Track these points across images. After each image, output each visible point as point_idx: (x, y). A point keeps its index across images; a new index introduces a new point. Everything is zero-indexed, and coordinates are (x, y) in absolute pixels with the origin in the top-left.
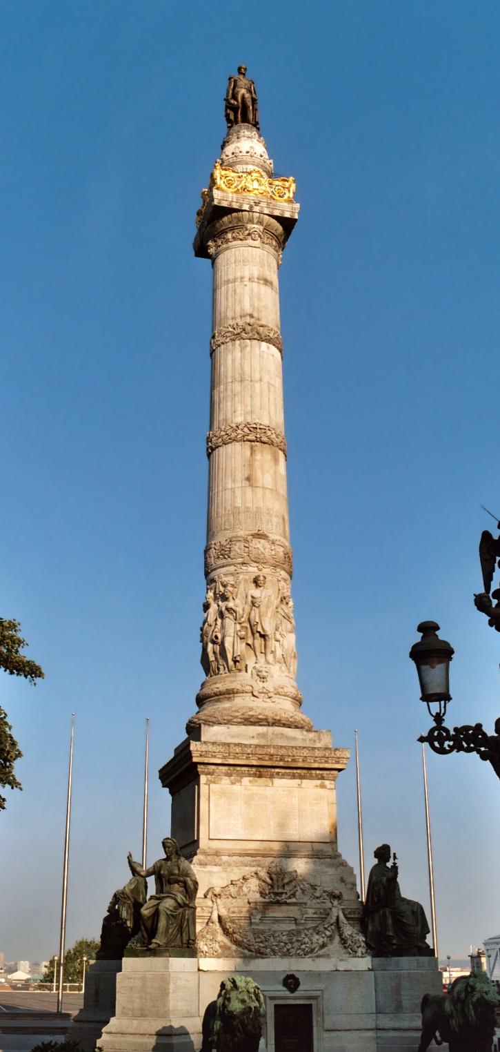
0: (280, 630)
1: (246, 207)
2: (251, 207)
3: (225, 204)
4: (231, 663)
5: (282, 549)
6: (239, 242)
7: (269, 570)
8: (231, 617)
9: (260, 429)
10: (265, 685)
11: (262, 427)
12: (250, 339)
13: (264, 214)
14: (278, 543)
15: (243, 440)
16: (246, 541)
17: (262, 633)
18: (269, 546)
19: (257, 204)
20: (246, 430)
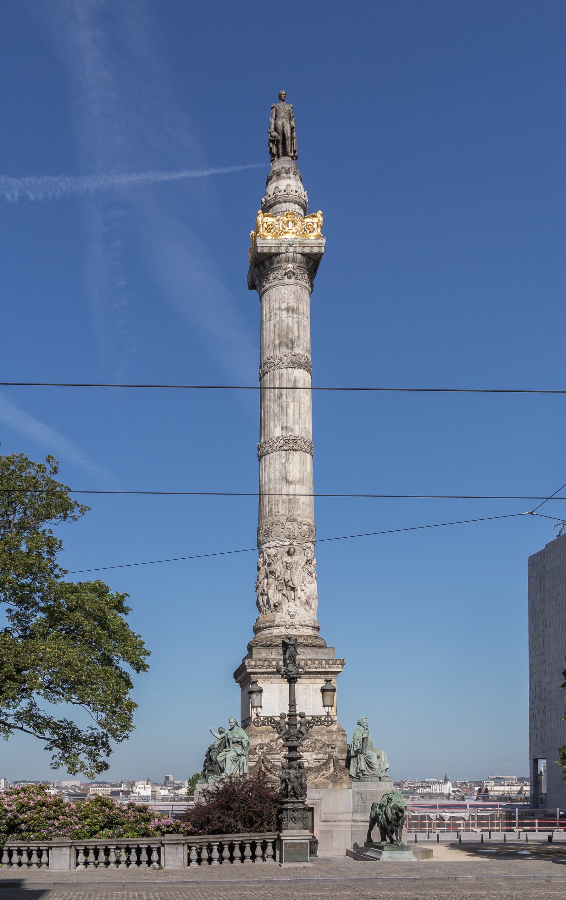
0: (305, 582)
4: (272, 607)
5: (307, 527)
6: (277, 282)
8: (273, 577)
10: (293, 620)
11: (293, 438)
14: (303, 523)
15: (281, 448)
16: (282, 524)
17: (292, 586)
20: (282, 441)
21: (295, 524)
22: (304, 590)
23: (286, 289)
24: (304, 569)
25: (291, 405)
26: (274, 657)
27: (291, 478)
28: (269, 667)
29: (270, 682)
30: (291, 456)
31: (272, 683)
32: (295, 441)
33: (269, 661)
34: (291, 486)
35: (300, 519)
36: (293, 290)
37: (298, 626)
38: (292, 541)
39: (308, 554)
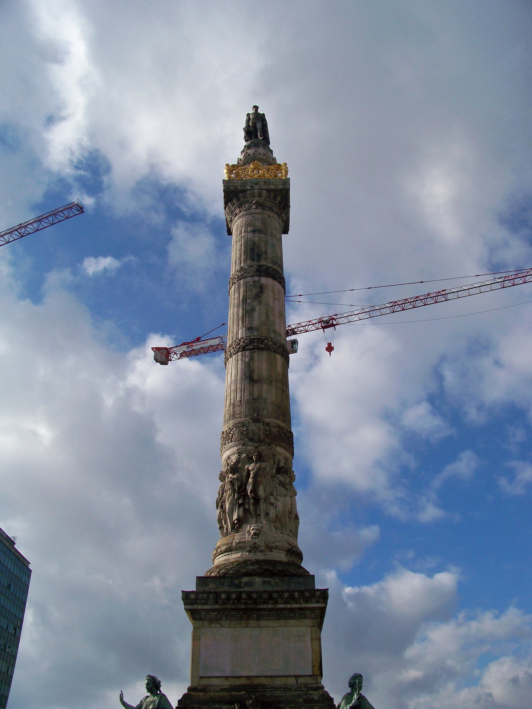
0: (275, 493)
1: (249, 187)
2: (252, 187)
3: (232, 188)
5: (276, 430)
7: (264, 447)
9: (258, 339)
10: (257, 541)
11: (259, 337)
12: (252, 277)
13: (262, 190)
14: (272, 424)
18: (264, 428)
19: (257, 184)
21: (260, 425)
22: (273, 504)
23: (253, 217)
24: (274, 479)
25: (257, 308)
26: (226, 589)
27: (255, 377)
28: (217, 603)
29: (219, 626)
30: (255, 355)
31: (222, 626)
32: (260, 340)
33: (216, 593)
34: (256, 386)
35: (267, 420)
36: (260, 217)
37: (263, 548)
38: (256, 445)
39: (279, 461)
